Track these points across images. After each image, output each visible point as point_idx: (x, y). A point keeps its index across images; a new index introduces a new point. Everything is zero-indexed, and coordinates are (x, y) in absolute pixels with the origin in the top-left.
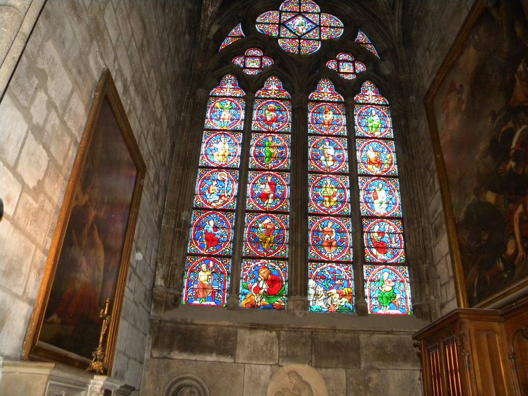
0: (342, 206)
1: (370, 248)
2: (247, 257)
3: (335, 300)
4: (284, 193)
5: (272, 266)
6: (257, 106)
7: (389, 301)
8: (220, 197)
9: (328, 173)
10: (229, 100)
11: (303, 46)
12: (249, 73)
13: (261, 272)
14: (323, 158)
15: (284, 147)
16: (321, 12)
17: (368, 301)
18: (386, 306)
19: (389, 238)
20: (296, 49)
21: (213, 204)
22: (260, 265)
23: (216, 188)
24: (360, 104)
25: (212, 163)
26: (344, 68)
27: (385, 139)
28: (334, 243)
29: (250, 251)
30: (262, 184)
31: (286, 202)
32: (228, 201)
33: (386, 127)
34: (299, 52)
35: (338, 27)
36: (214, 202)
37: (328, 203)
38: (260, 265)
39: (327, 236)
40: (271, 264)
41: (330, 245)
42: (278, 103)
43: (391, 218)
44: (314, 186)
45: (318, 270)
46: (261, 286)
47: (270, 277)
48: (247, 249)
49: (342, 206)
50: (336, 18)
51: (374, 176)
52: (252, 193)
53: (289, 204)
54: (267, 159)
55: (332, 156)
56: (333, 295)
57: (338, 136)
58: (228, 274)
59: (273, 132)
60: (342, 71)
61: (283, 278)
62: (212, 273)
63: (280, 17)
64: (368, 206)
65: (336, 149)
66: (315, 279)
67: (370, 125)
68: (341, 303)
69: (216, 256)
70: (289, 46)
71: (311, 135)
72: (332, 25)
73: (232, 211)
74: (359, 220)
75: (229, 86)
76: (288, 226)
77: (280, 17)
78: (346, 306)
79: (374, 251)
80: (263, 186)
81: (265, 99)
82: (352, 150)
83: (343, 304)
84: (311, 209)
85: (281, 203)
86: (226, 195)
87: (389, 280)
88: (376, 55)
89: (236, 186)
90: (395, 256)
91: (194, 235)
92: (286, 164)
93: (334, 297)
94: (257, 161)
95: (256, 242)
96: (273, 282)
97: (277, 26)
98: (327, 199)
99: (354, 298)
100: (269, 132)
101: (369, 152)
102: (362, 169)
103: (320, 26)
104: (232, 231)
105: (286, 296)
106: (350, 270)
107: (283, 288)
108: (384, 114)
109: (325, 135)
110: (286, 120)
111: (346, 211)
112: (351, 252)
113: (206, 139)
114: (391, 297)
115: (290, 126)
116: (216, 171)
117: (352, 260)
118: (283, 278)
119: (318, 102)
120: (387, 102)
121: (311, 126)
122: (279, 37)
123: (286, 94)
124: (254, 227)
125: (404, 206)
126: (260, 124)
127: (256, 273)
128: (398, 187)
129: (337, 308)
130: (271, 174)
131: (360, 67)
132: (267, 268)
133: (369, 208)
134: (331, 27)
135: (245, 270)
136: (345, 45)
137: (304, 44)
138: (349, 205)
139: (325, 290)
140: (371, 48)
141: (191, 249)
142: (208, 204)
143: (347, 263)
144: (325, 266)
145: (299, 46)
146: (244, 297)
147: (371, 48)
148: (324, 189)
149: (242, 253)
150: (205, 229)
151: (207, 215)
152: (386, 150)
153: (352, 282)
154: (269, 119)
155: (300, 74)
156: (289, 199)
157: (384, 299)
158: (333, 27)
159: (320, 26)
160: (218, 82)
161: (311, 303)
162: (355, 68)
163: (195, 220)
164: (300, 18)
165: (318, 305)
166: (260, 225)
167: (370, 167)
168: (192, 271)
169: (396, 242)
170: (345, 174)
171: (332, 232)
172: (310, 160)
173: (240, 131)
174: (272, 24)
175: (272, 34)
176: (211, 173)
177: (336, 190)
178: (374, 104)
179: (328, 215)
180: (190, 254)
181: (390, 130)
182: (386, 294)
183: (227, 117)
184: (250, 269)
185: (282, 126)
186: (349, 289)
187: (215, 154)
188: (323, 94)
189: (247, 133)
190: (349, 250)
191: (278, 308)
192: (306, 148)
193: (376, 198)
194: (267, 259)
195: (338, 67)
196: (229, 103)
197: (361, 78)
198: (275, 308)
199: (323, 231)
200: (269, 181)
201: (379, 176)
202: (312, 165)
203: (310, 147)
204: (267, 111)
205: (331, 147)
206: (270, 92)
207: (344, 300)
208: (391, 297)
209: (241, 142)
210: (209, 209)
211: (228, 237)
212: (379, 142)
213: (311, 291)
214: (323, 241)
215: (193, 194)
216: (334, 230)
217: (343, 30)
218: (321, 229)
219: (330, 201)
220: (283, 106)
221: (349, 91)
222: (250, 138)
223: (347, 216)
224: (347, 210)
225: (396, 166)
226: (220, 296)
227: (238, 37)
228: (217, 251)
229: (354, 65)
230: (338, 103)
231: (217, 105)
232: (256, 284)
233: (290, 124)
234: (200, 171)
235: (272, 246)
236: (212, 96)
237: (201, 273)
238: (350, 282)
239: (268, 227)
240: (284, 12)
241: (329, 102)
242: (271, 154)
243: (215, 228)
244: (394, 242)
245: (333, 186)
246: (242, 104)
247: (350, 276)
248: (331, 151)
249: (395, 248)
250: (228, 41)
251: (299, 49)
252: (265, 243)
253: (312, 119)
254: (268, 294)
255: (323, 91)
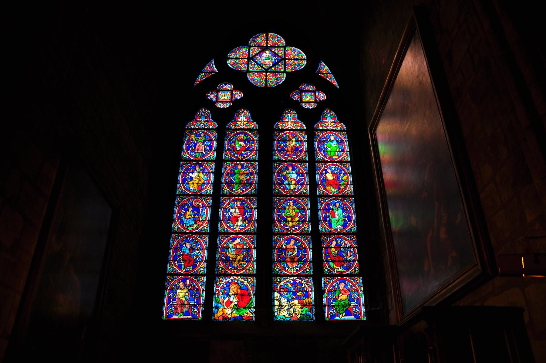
0: (303, 226)
1: (328, 261)
2: (219, 275)
3: (297, 310)
4: (251, 216)
5: (241, 282)
6: (228, 137)
7: (345, 309)
8: (196, 223)
9: (291, 196)
10: (202, 132)
11: (269, 78)
12: (220, 106)
13: (232, 288)
14: (286, 182)
15: (252, 174)
16: (287, 45)
17: (326, 309)
18: (343, 314)
19: (345, 252)
20: (263, 81)
21: (190, 228)
22: (230, 281)
23: (191, 213)
24: (320, 130)
25: (189, 190)
26: (306, 98)
27: (341, 162)
28: (296, 259)
29: (222, 269)
30: (232, 208)
31: (254, 224)
32: (202, 225)
33: (343, 151)
34: (266, 84)
35: (301, 59)
36: (190, 226)
37: (290, 223)
38: (230, 281)
39: (290, 253)
40: (240, 280)
41: (292, 260)
42: (247, 134)
43: (347, 234)
44: (278, 209)
45: (282, 283)
46: (231, 300)
47: (239, 291)
48: (220, 267)
49: (303, 226)
50: (299, 50)
51: (332, 196)
52: (224, 216)
53: (256, 225)
54: (236, 186)
55: (295, 180)
56: (295, 305)
57: (299, 161)
58: (203, 290)
59: (242, 160)
60: (304, 100)
61: (251, 292)
62: (189, 290)
63: (249, 52)
64: (326, 224)
65: (298, 174)
66: (279, 292)
67: (329, 149)
68: (302, 312)
69: (192, 275)
70: (257, 79)
71: (275, 161)
72: (296, 57)
73: (206, 234)
74: (317, 236)
75: (203, 119)
76: (256, 246)
77: (249, 52)
78: (307, 315)
79: (332, 264)
80: (232, 210)
81: (236, 130)
82: (312, 174)
83: (304, 313)
84: (276, 228)
85: (249, 225)
86: (201, 219)
87: (345, 289)
88: (335, 83)
89: (209, 211)
90: (350, 268)
91: (174, 257)
92: (253, 189)
93: (296, 307)
94: (228, 188)
95: (227, 260)
96: (243, 295)
97: (246, 60)
98: (289, 219)
99: (314, 307)
100: (238, 160)
101: (327, 175)
102: (321, 190)
103: (285, 59)
104: (206, 252)
105: (254, 308)
106: (310, 282)
107: (251, 301)
108: (341, 138)
109: (289, 161)
110: (254, 148)
111: (306, 229)
112: (312, 266)
113: (182, 169)
114: (346, 305)
115: (258, 154)
116: (191, 198)
117: (312, 273)
118: (251, 292)
119: (283, 130)
120: (345, 128)
121: (275, 153)
122: (248, 71)
123: (254, 125)
124: (224, 247)
125: (358, 223)
126: (230, 154)
127: (227, 288)
128: (354, 205)
129: (299, 316)
130: (241, 199)
131: (322, 96)
132: (237, 283)
133: (327, 225)
134: (294, 59)
135: (218, 286)
136: (308, 75)
137: (270, 76)
138: (310, 224)
139: (288, 300)
140: (331, 79)
141: (171, 268)
142: (184, 228)
143: (307, 276)
144: (288, 280)
145: (266, 79)
146: (216, 310)
147: (331, 79)
148: (287, 211)
149: (215, 271)
150: (182, 251)
151: (184, 238)
152: (343, 172)
153: (312, 294)
154: (238, 148)
155: (267, 104)
156: (256, 221)
157: (341, 307)
158: (297, 58)
159: (285, 59)
160: (193, 117)
161: (276, 313)
162: (315, 97)
163: (173, 243)
164: (268, 52)
165: (283, 315)
166: (231, 246)
167: (328, 188)
168: (171, 290)
169: (351, 256)
170: (306, 196)
171: (294, 249)
172: (275, 184)
173: (212, 161)
174: (242, 59)
175: (241, 68)
176: (188, 200)
177: (298, 211)
178: (333, 130)
179: (291, 234)
180: (170, 274)
181: (346, 154)
182: (343, 302)
183: (201, 148)
184: (221, 285)
185: (250, 154)
186: (309, 299)
187: (190, 183)
188: (287, 123)
189: (219, 162)
190: (309, 264)
191: (247, 319)
192: (271, 173)
193: (333, 216)
194: (237, 276)
195: (301, 97)
196: (202, 135)
197: (321, 106)
198: (244, 319)
199: (287, 249)
200: (239, 205)
201: (336, 196)
202: (276, 189)
203: (275, 173)
204: (237, 141)
205: (294, 172)
206: (239, 123)
207: (305, 309)
208: (346, 305)
209: (213, 171)
210: (186, 233)
211: (203, 257)
212: (337, 165)
213: (276, 303)
214: (286, 258)
215: (172, 220)
216: (296, 247)
217: (306, 61)
218: (284, 247)
219: (292, 221)
220: (251, 136)
221: (310, 118)
222: (222, 166)
223: (308, 234)
224: (308, 228)
225: (352, 186)
226: (196, 310)
227: (210, 72)
228: (193, 269)
229: (315, 94)
230: (300, 130)
231: (193, 137)
232: (227, 299)
233: (257, 152)
234: (178, 198)
235: (241, 264)
236: (188, 129)
237: (179, 291)
238: (310, 293)
239: (238, 247)
240: (252, 46)
241: (292, 130)
242: (240, 181)
243: (192, 249)
244: (349, 255)
245: (295, 207)
246: (214, 136)
247: (311, 288)
248: (294, 176)
249: (350, 261)
250: (202, 77)
251: (266, 81)
252: (235, 261)
253: (277, 147)
254: (238, 307)
255: (287, 120)
